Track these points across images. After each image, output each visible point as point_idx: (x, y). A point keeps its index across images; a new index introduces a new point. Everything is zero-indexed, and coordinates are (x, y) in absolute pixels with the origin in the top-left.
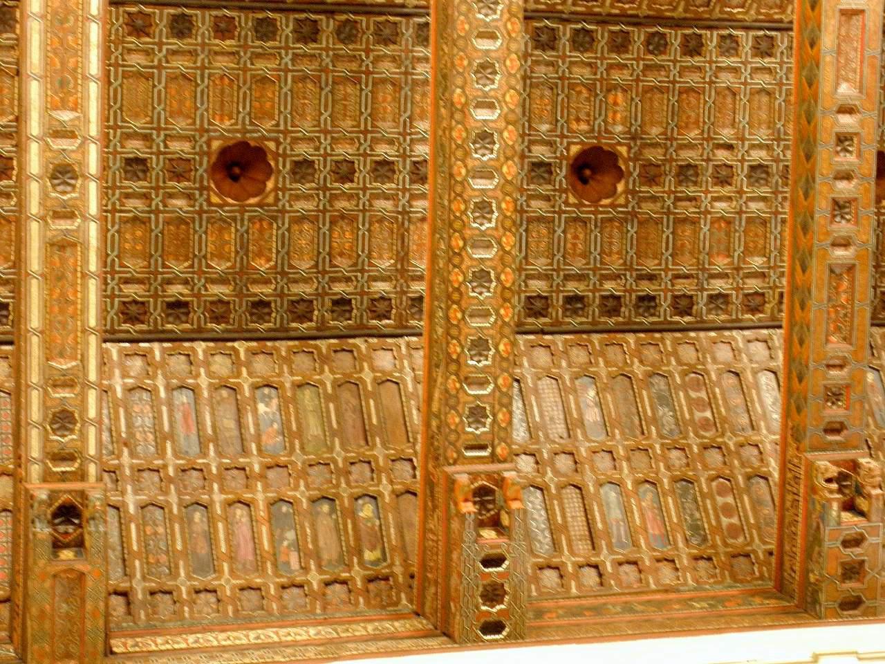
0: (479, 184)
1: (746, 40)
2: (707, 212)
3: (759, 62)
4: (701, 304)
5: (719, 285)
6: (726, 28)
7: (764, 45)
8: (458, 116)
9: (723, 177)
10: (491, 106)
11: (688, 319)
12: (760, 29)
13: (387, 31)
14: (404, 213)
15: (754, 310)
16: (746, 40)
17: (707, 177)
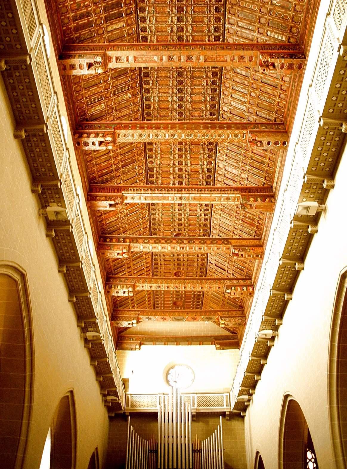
2: (191, 34)
3: (148, 21)
4: (217, 34)
5: (212, 29)
6: (139, 31)
7: (143, 20)
8: (167, 141)
9: (181, 29)
10: (165, 134)
11: (221, 37)
13: (148, 107)
14: (190, 102)
15: (220, 19)
16: (142, 25)
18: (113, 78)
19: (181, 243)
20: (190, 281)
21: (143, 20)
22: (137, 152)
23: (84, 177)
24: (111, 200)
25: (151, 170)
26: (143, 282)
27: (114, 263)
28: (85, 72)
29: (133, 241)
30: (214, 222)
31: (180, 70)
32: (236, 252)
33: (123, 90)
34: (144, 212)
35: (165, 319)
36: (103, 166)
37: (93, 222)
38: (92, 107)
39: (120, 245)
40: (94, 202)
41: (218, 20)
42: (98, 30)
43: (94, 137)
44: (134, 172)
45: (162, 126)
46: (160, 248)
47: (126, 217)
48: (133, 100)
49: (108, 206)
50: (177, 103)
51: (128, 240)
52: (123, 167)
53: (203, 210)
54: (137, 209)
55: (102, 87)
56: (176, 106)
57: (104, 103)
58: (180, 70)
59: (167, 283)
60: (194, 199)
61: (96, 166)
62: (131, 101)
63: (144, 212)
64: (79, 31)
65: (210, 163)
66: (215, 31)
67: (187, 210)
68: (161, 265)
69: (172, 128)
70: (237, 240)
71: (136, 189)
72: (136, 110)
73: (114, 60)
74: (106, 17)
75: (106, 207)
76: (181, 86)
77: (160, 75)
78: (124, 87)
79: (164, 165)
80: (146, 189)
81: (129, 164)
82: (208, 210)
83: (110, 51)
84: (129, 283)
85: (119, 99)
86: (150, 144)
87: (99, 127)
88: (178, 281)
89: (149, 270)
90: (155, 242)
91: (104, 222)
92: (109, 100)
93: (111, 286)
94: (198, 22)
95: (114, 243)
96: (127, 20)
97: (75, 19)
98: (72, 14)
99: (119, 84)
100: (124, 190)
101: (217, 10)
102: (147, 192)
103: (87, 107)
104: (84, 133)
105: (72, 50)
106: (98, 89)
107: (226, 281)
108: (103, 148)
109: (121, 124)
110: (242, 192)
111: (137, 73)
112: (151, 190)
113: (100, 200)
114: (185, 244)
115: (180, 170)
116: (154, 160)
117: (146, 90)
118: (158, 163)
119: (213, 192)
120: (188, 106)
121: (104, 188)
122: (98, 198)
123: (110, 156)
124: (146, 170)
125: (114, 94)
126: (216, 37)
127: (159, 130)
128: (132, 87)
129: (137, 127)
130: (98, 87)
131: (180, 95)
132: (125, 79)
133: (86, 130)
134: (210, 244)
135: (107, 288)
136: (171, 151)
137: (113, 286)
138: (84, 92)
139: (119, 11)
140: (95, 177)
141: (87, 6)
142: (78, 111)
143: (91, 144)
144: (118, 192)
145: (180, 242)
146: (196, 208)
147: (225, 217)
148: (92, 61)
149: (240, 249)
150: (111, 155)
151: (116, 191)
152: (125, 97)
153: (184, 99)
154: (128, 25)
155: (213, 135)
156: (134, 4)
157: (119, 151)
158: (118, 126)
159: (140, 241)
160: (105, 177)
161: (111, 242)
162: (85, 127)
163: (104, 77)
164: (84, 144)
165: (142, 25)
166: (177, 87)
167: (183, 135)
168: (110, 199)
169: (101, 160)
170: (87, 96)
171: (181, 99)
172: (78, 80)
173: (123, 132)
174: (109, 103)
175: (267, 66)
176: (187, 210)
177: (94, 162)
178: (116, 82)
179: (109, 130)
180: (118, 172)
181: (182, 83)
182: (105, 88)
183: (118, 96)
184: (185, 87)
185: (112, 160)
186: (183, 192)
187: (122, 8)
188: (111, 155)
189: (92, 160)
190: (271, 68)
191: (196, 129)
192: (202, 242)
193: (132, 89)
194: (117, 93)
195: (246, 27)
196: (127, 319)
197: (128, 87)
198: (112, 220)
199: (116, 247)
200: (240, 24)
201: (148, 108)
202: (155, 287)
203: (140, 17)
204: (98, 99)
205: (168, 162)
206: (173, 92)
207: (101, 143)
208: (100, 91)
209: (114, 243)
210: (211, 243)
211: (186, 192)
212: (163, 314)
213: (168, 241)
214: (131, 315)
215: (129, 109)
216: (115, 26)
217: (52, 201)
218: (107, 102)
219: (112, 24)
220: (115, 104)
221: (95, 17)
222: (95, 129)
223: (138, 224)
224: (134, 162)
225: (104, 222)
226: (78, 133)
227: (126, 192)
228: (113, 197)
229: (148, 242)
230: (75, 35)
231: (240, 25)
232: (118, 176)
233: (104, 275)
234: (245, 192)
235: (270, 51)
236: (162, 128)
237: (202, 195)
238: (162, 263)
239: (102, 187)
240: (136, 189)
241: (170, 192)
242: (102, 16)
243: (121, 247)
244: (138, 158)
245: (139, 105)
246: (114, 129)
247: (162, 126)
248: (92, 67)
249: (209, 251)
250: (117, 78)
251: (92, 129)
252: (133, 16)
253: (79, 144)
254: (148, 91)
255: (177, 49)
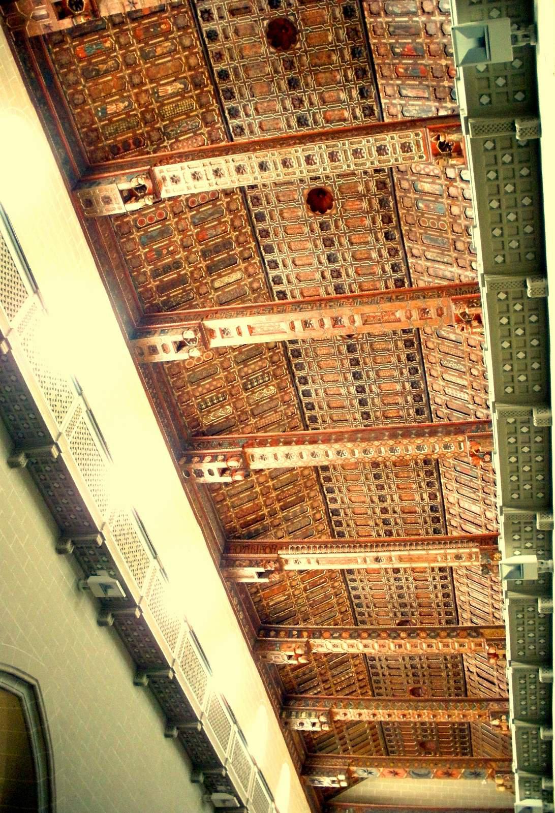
0: (357, 455)
1: (272, 273)
2: (355, 279)
4: (398, 276)
5: (388, 268)
6: (270, 283)
7: (273, 265)
9: (337, 274)
10: (326, 452)
11: (406, 280)
12: (265, 268)
14: (378, 395)
15: (397, 251)
17: (339, 281)
18: (238, 363)
19: (395, 638)
20: (427, 704)
21: (273, 265)
22: (305, 483)
23: (211, 529)
24: (258, 566)
25: (336, 512)
26: (345, 707)
27: (296, 673)
28: (173, 356)
29: (314, 634)
30: (461, 598)
31: (350, 342)
32: (492, 651)
33: (261, 381)
34: (336, 584)
35: (396, 774)
36: (247, 509)
37: (240, 603)
38: (209, 412)
39: (292, 642)
40: (231, 570)
41: (393, 252)
42: (198, 288)
43: (210, 462)
44: (304, 517)
45: (320, 438)
46: (361, 646)
47: (305, 595)
48: (282, 396)
49: (256, 576)
50: (356, 397)
51: (305, 634)
52: (283, 509)
53: (437, 578)
54: (323, 580)
55: (221, 378)
56: (356, 403)
57: (229, 404)
58: (350, 342)
59: (385, 708)
60: (401, 559)
61: (234, 510)
62: (277, 398)
63: (336, 584)
64: (166, 291)
65: (433, 497)
66: (394, 271)
67: (411, 579)
68: (384, 675)
69: (336, 441)
70: (493, 630)
71: (300, 546)
72: (290, 414)
73: (218, 333)
74: (208, 267)
75: (252, 577)
76: (356, 369)
77: (319, 353)
78: (261, 375)
79: (356, 504)
80: (318, 546)
81: (293, 504)
82: (446, 578)
83: (209, 320)
84: (322, 708)
85: (256, 397)
86: (325, 468)
87: (220, 445)
88: (405, 705)
89: (365, 686)
90: (351, 637)
91: (264, 603)
92: (238, 399)
93: (291, 712)
94: (361, 259)
95: (281, 639)
96: (246, 268)
97: (156, 274)
98: (150, 267)
99: (250, 371)
100: (281, 548)
101: (388, 237)
102: (318, 551)
103: (201, 412)
104: (197, 455)
105: (152, 324)
106: (215, 383)
107: (491, 703)
108: (227, 479)
109: (255, 438)
110: (481, 545)
111: (279, 352)
112: (326, 547)
113: (240, 566)
114: (402, 639)
115: (384, 511)
116: (337, 495)
117: (300, 378)
118: (346, 500)
119: (430, 547)
120: (376, 400)
121: (248, 546)
122: (237, 563)
123: (256, 492)
124: (327, 513)
125: (246, 390)
126: (396, 281)
127: (315, 446)
128: (275, 376)
129: (280, 442)
130: (214, 380)
131: (358, 383)
132: (260, 363)
133: (198, 450)
134: (445, 637)
135: (284, 716)
136: (363, 478)
137: (294, 713)
138: (190, 388)
139: (229, 255)
140: (234, 527)
141: (172, 253)
142: (185, 420)
143: (206, 473)
144: (271, 553)
145: (393, 635)
146: (426, 575)
147: (476, 588)
148: (179, 338)
149: (498, 645)
150: (258, 489)
151: (268, 550)
152: (266, 393)
153: (367, 390)
154: (249, 276)
155: (432, 446)
156: (254, 241)
157: (270, 483)
158: (250, 442)
159: (327, 634)
160: (253, 528)
161: (277, 637)
162: (198, 445)
163: (222, 363)
164: (195, 473)
165: (272, 273)
166: (350, 370)
167: (356, 452)
168: (257, 564)
169: (241, 499)
170: (198, 394)
171: (360, 390)
172: (177, 370)
173: (257, 451)
174: (239, 405)
175: (469, 322)
176: (411, 579)
177: (228, 502)
178: (246, 369)
179: (235, 450)
180: (275, 518)
181: (358, 363)
182: (227, 380)
183: (253, 393)
184: (363, 369)
185: (261, 500)
186: (379, 549)
187: (233, 250)
188: (258, 489)
189: (224, 500)
190: (475, 323)
191: (377, 439)
192: (433, 634)
193: (276, 379)
194: (250, 386)
195: (439, 259)
196: (329, 773)
197: (269, 377)
198: (278, 600)
199: (285, 646)
200: (429, 255)
201: (311, 410)
202: (382, 715)
203: (268, 261)
204: (218, 398)
205: (363, 499)
206: (346, 379)
207: (223, 472)
208: (219, 385)
209: (281, 639)
210: (449, 636)
211: (385, 549)
212: (392, 765)
213: (373, 635)
214: (336, 765)
215: (276, 412)
216: (226, 280)
217: (99, 566)
218: (234, 403)
219: (220, 276)
220: (250, 405)
221: (190, 267)
222: (213, 448)
223: (330, 606)
224: (302, 500)
225: (264, 603)
226: (186, 456)
227: (284, 552)
228: (262, 561)
229: (340, 637)
230: (159, 300)
231: (429, 257)
232: (278, 525)
233: (275, 694)
234: (488, 544)
235: (469, 295)
236: (320, 442)
237: (412, 553)
238: (387, 673)
239: (244, 544)
240: (300, 546)
241: (358, 550)
242: (200, 265)
243: (294, 645)
244: (308, 494)
245: (294, 405)
246: (243, 447)
247: (320, 438)
248: (185, 348)
249: (462, 650)
250: (245, 362)
251: (208, 449)
252: (257, 259)
253: (188, 474)
254: (304, 380)
255: (315, 308)
